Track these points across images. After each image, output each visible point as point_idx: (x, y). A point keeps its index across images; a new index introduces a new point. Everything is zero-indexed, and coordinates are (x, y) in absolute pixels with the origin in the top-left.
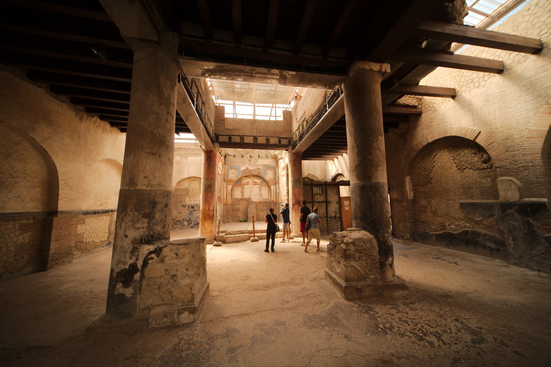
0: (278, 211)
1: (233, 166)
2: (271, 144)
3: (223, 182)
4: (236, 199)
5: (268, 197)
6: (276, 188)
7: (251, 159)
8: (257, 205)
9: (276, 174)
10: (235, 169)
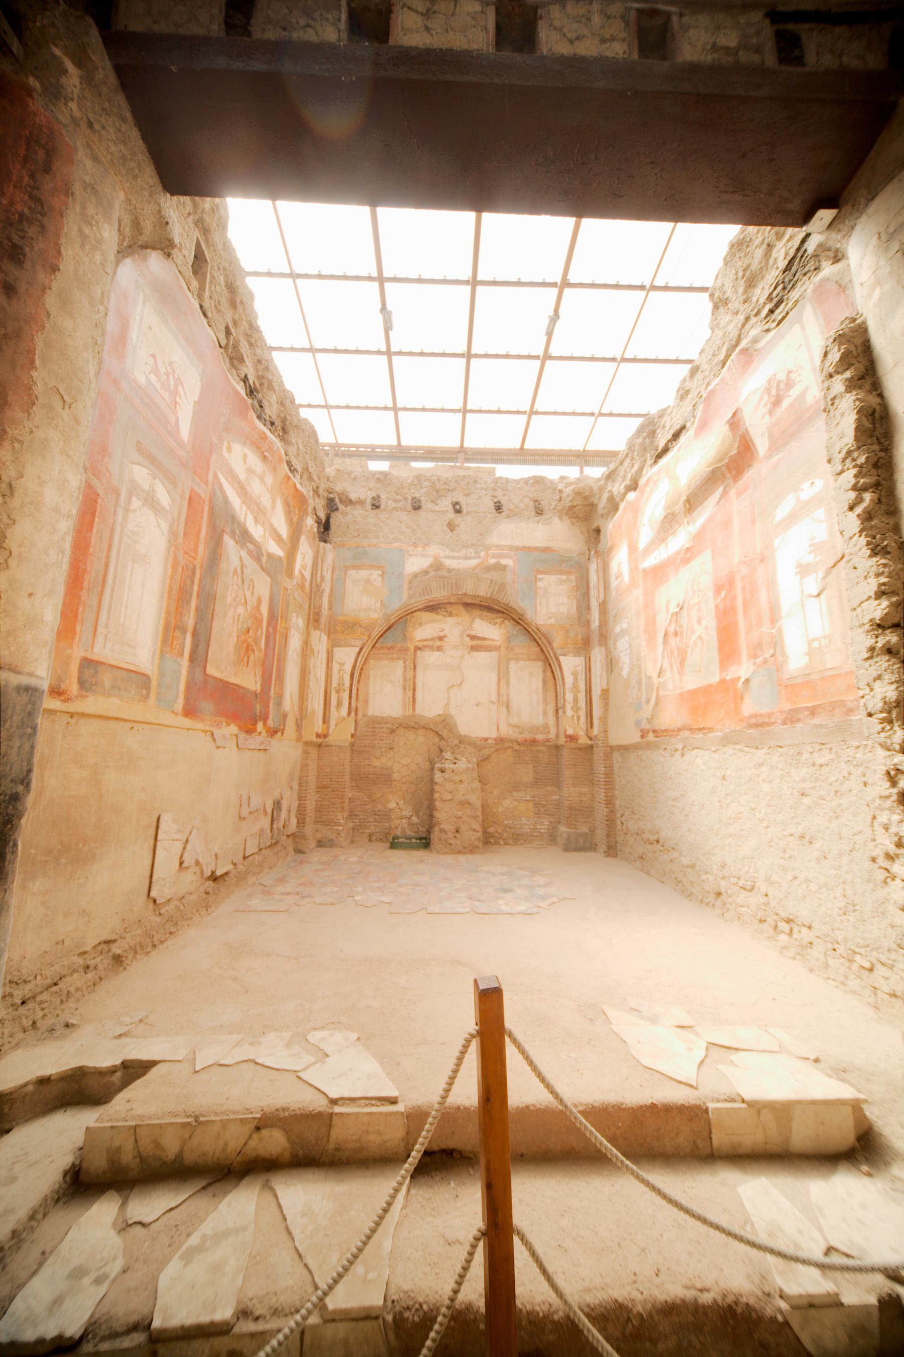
0: (601, 795)
3: (298, 622)
4: (377, 722)
5: (545, 714)
6: (588, 669)
7: (458, 519)
8: (486, 759)
9: (586, 595)
10: (378, 567)
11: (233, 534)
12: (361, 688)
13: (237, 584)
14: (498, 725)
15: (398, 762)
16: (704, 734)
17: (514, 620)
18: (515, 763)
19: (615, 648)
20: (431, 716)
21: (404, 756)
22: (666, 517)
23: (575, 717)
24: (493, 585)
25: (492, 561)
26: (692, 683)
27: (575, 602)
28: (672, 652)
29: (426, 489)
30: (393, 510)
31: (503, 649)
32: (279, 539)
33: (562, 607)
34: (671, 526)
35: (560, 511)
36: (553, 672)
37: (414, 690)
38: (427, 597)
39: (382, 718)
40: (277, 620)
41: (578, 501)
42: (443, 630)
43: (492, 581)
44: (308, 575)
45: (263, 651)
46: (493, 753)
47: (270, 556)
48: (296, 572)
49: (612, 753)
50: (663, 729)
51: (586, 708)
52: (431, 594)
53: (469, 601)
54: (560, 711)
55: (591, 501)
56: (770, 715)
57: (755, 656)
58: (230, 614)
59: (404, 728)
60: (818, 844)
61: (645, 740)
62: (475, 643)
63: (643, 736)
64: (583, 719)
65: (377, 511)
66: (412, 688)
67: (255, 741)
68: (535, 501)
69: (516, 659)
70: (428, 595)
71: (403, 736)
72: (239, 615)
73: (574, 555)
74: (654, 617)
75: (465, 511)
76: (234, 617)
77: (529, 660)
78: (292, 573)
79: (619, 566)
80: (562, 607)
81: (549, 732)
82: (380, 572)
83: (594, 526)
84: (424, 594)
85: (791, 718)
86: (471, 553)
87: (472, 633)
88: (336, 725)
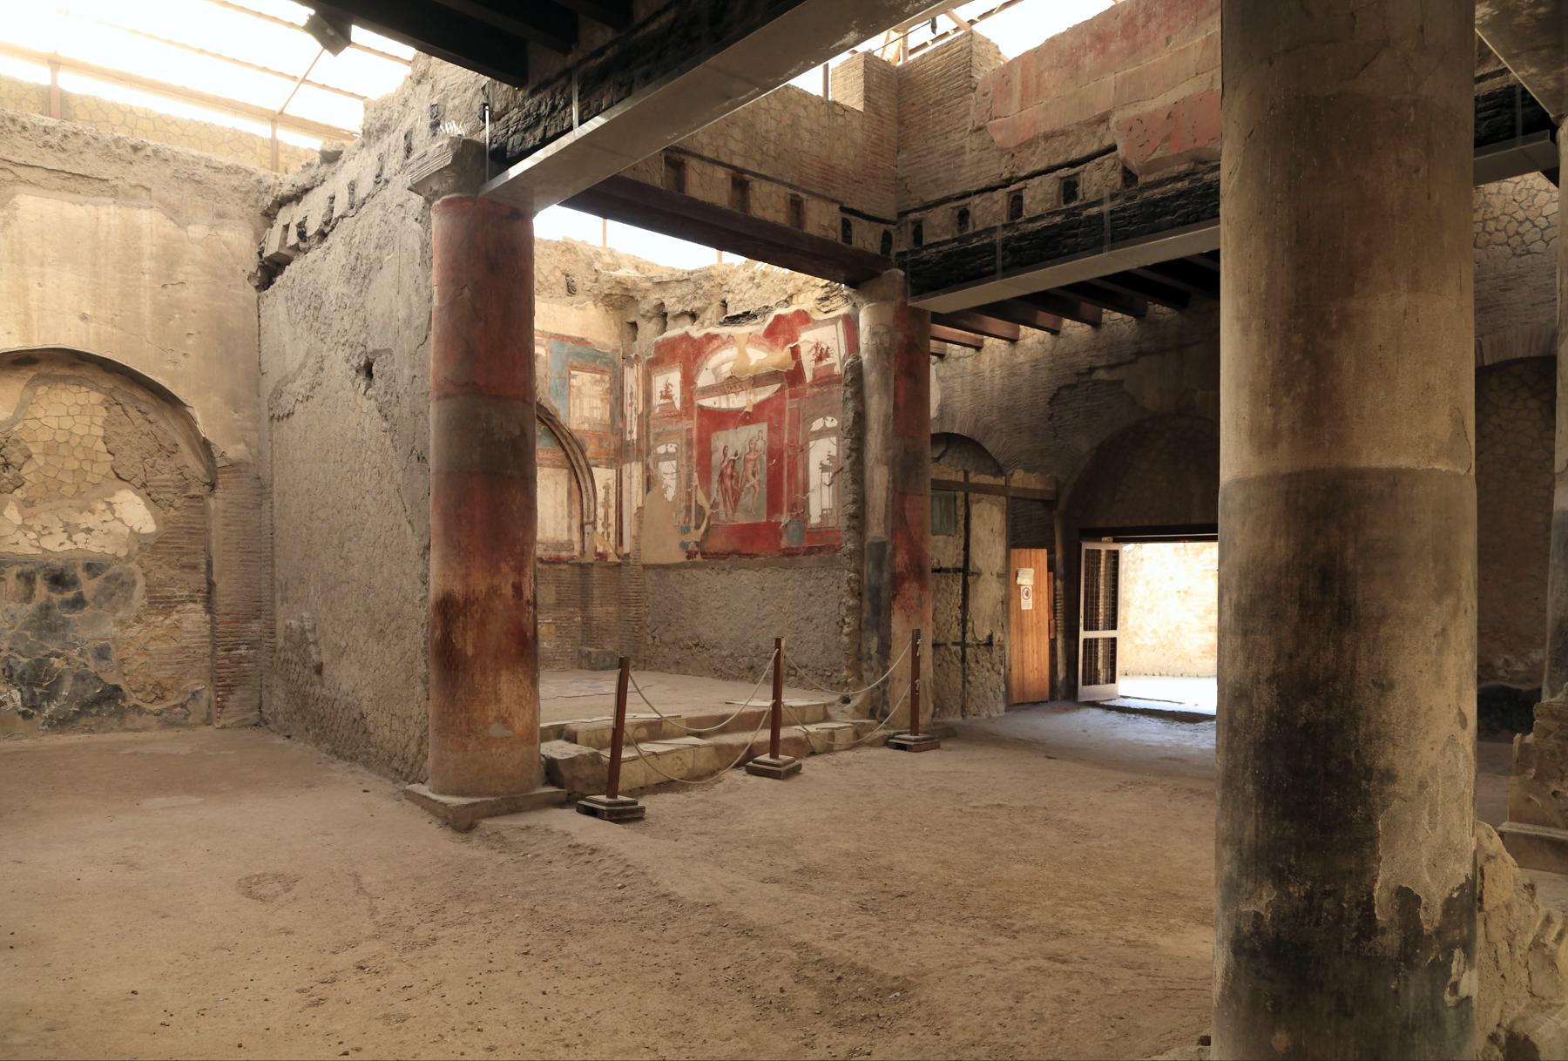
2: (810, 237)
19: (656, 466)
22: (731, 377)
26: (742, 519)
27: (608, 406)
28: (726, 490)
35: (595, 296)
36: (578, 482)
41: (617, 291)
54: (588, 528)
56: (797, 549)
57: (792, 511)
60: (815, 621)
63: (688, 557)
64: (612, 536)
68: (567, 276)
73: (608, 351)
83: (632, 319)
85: (810, 551)
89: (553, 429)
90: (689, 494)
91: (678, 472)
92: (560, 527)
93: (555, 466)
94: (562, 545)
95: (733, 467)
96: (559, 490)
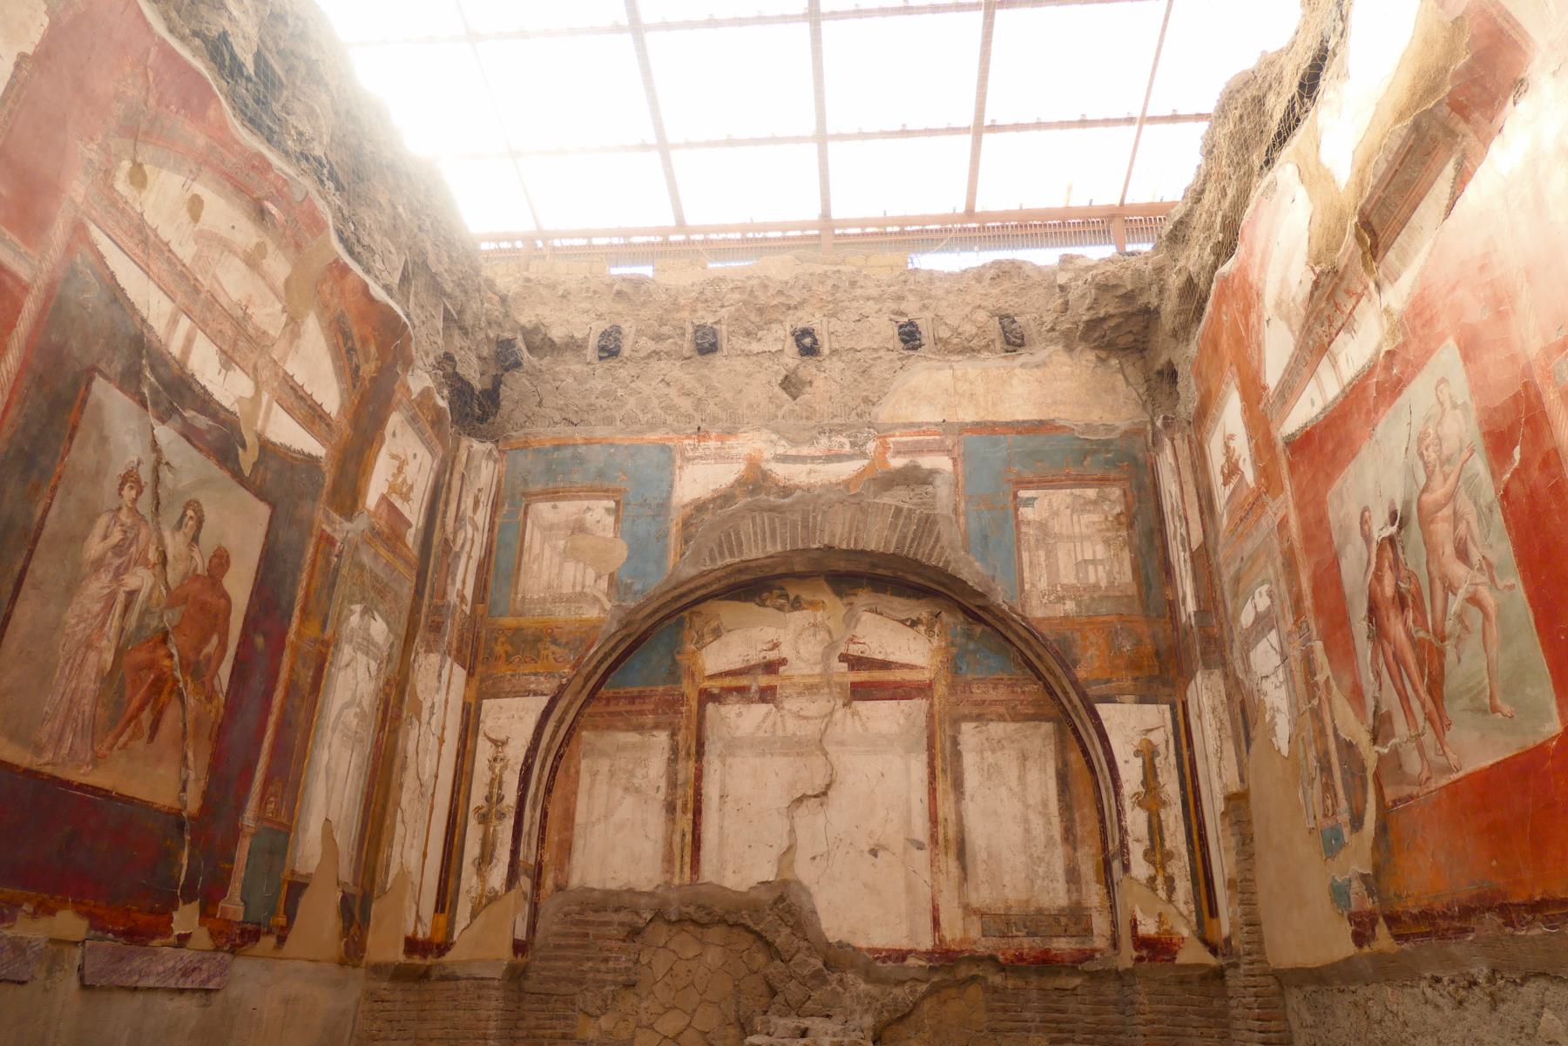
1: (579, 460)
5: (1073, 875)
6: (1183, 734)
7: (808, 369)
10: (606, 493)
11: (129, 381)
12: (555, 812)
13: (134, 511)
14: (935, 910)
15: (650, 1027)
16: (1549, 922)
17: (966, 611)
18: (994, 1031)
19: (1248, 669)
20: (743, 888)
21: (667, 1010)
22: (1316, 284)
23: (1160, 880)
24: (901, 521)
25: (897, 463)
27: (1126, 555)
28: (1399, 660)
29: (733, 309)
30: (649, 356)
31: (941, 689)
32: (312, 415)
33: (1091, 568)
34: (1337, 306)
36: (1085, 752)
37: (698, 812)
38: (729, 560)
39: (608, 893)
40: (290, 616)
42: (776, 646)
43: (899, 511)
44: (414, 512)
45: (222, 697)
46: (924, 997)
47: (266, 447)
48: (372, 499)
49: (1281, 995)
50: (1415, 911)
51: (1191, 852)
52: (741, 552)
53: (842, 566)
55: (1142, 300)
58: (98, 586)
59: (669, 922)
61: (1366, 949)
62: (863, 676)
63: (1360, 938)
64: (1183, 887)
65: (612, 363)
66: (690, 805)
67: (163, 960)
69: (979, 718)
70: (732, 555)
71: (665, 947)
72: (132, 595)
74: (1335, 563)
75: (826, 350)
76: (112, 597)
77: (1013, 720)
78: (355, 502)
79: (1227, 447)
80: (1091, 568)
81: (1088, 931)
82: (612, 504)
83: (1160, 363)
84: (722, 554)
86: (842, 445)
87: (854, 650)
88: (474, 916)
89: (1001, 628)
90: (1316, 714)
91: (1284, 658)
92: (1041, 871)
93: (1017, 717)
94: (1056, 918)
95: (1396, 565)
96: (1033, 775)
